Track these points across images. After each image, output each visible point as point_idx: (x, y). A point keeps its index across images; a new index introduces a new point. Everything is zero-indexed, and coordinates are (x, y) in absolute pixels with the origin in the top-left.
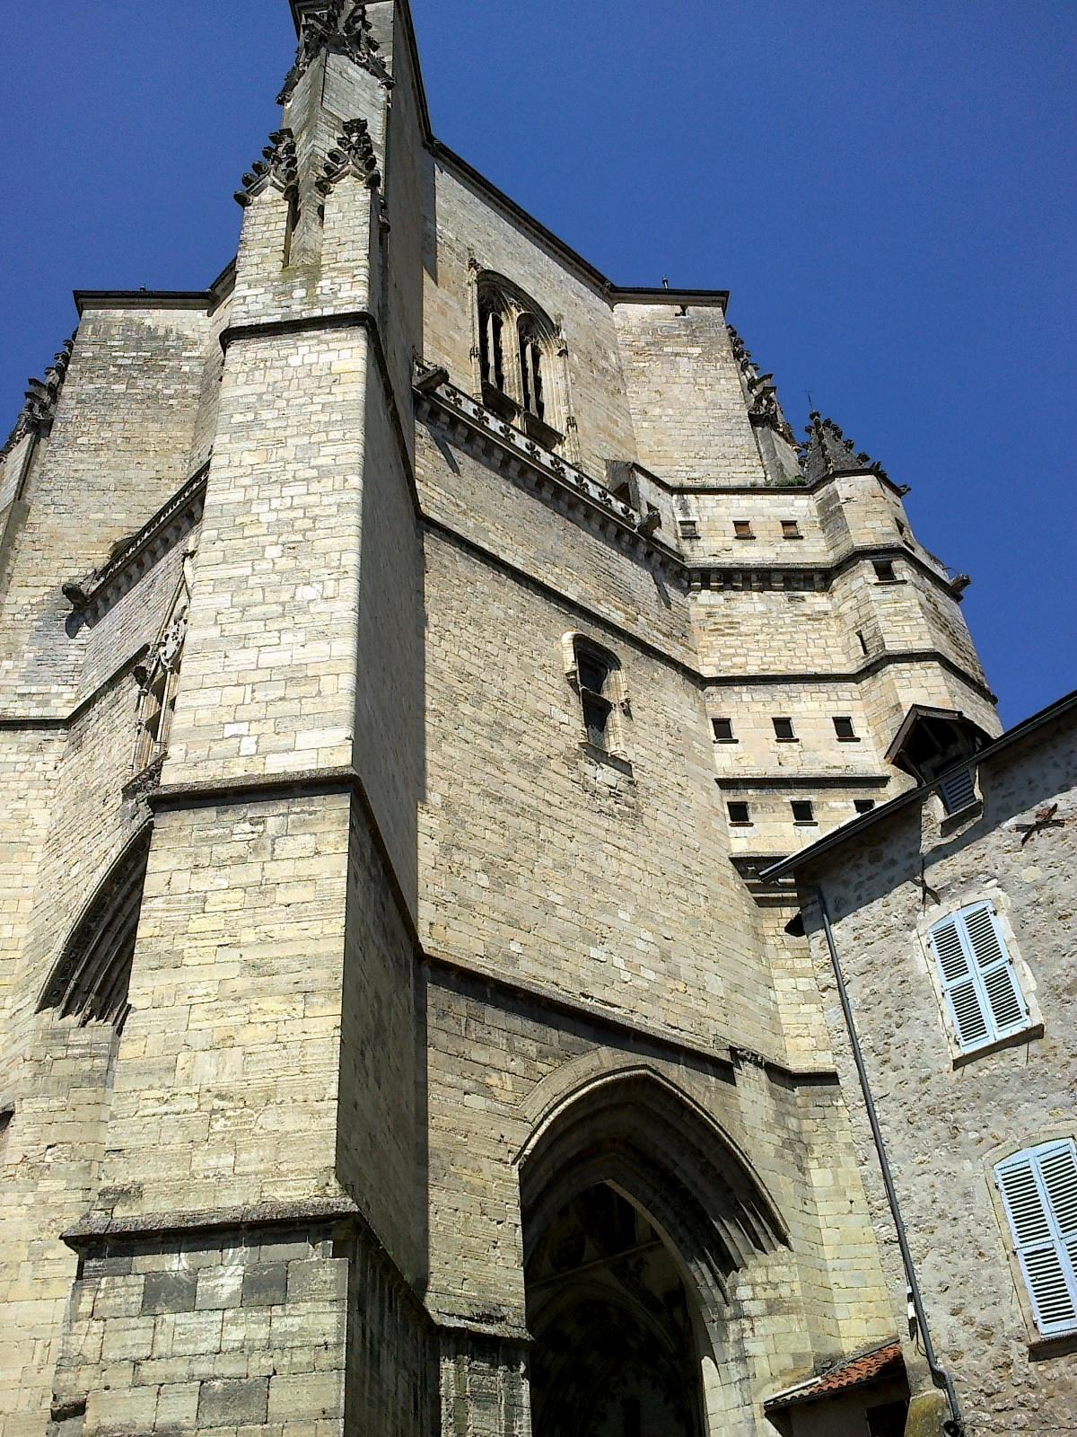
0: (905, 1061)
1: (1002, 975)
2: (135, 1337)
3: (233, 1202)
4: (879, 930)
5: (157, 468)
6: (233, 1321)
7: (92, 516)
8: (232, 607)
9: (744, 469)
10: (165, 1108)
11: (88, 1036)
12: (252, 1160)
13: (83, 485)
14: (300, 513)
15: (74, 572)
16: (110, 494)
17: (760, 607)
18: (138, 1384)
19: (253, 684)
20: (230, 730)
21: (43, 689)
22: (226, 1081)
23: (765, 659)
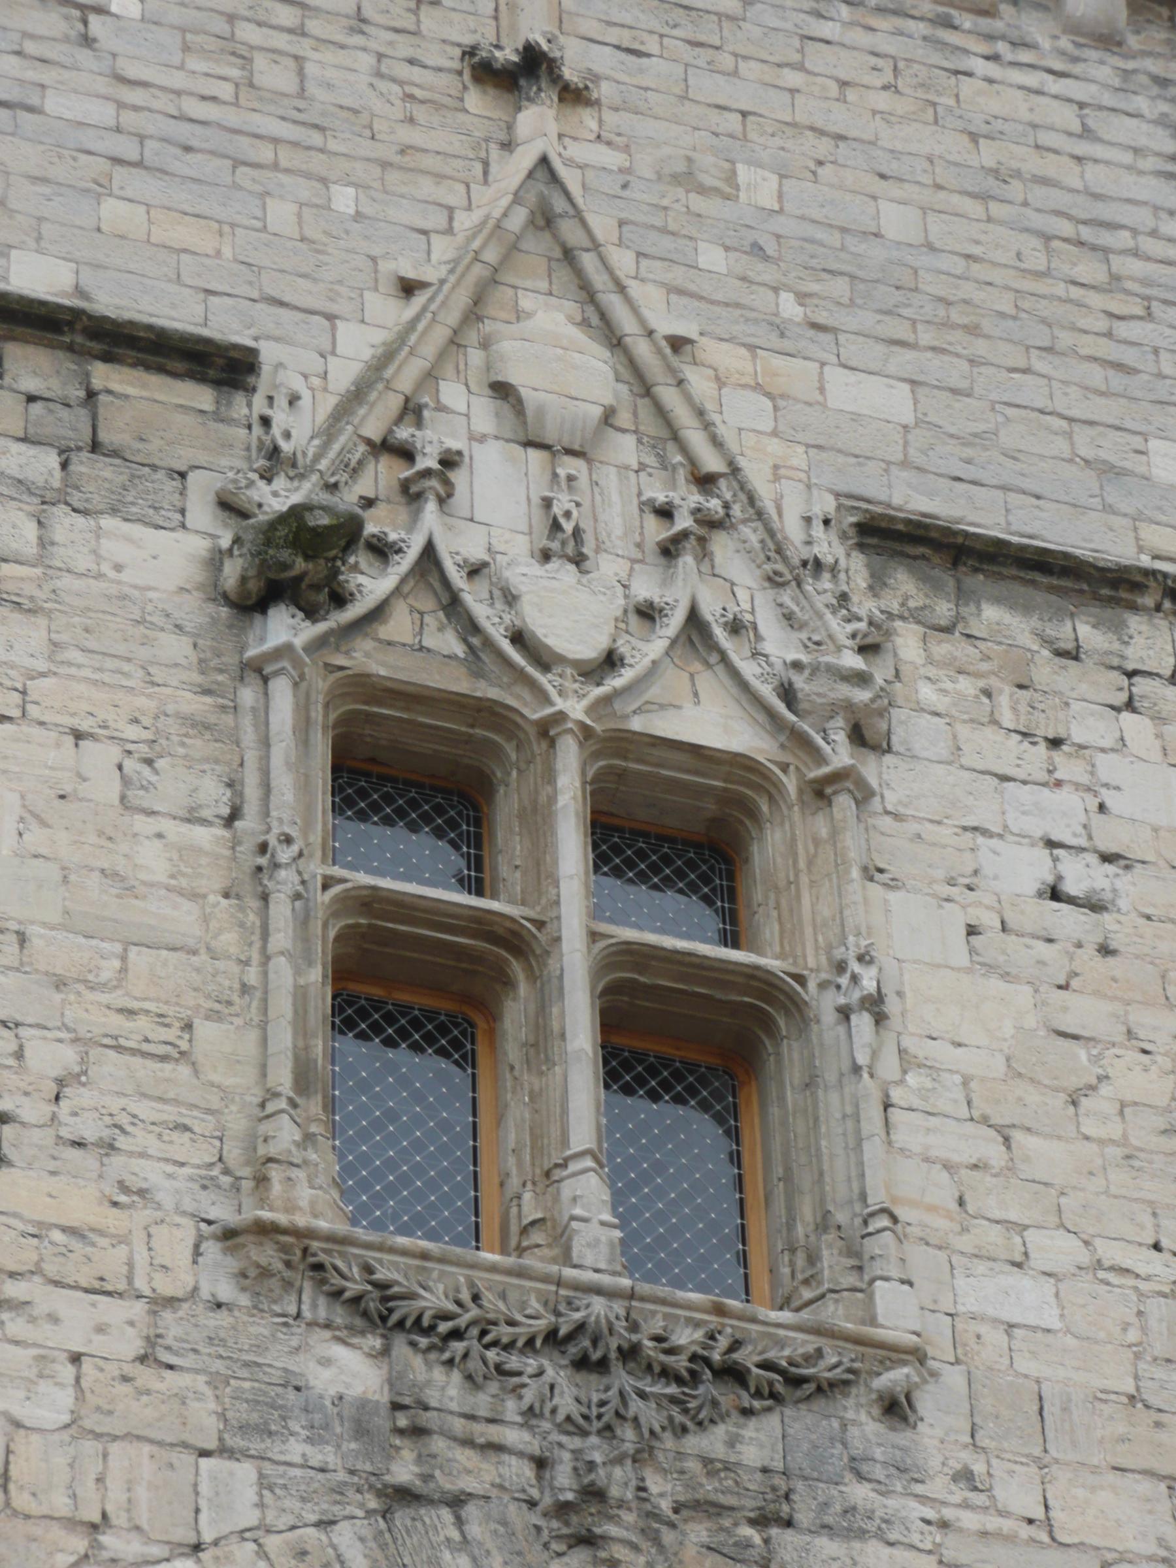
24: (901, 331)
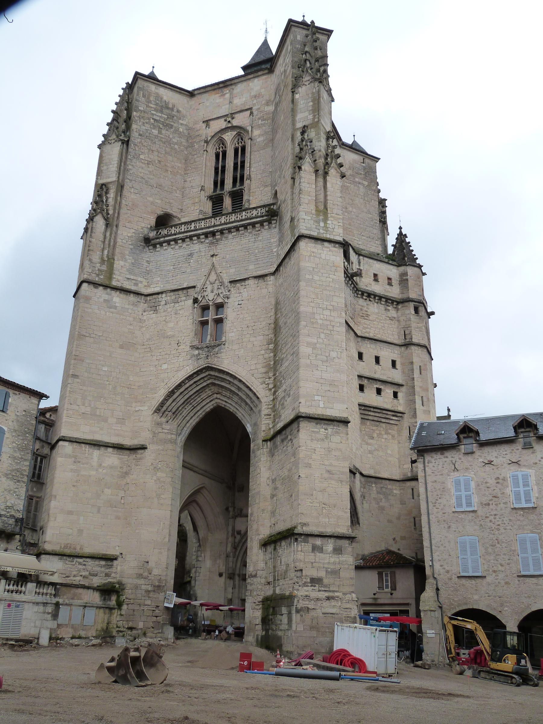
0: (440, 508)
1: (470, 496)
2: (311, 557)
3: (329, 531)
4: (440, 473)
5: (172, 180)
6: (332, 557)
7: (148, 198)
8: (313, 354)
9: (375, 245)
10: (311, 505)
11: (169, 426)
14: (328, 323)
16: (154, 189)
17: (376, 311)
18: (313, 567)
20: (316, 398)
21: (135, 278)
23: (375, 332)
24: (235, 264)
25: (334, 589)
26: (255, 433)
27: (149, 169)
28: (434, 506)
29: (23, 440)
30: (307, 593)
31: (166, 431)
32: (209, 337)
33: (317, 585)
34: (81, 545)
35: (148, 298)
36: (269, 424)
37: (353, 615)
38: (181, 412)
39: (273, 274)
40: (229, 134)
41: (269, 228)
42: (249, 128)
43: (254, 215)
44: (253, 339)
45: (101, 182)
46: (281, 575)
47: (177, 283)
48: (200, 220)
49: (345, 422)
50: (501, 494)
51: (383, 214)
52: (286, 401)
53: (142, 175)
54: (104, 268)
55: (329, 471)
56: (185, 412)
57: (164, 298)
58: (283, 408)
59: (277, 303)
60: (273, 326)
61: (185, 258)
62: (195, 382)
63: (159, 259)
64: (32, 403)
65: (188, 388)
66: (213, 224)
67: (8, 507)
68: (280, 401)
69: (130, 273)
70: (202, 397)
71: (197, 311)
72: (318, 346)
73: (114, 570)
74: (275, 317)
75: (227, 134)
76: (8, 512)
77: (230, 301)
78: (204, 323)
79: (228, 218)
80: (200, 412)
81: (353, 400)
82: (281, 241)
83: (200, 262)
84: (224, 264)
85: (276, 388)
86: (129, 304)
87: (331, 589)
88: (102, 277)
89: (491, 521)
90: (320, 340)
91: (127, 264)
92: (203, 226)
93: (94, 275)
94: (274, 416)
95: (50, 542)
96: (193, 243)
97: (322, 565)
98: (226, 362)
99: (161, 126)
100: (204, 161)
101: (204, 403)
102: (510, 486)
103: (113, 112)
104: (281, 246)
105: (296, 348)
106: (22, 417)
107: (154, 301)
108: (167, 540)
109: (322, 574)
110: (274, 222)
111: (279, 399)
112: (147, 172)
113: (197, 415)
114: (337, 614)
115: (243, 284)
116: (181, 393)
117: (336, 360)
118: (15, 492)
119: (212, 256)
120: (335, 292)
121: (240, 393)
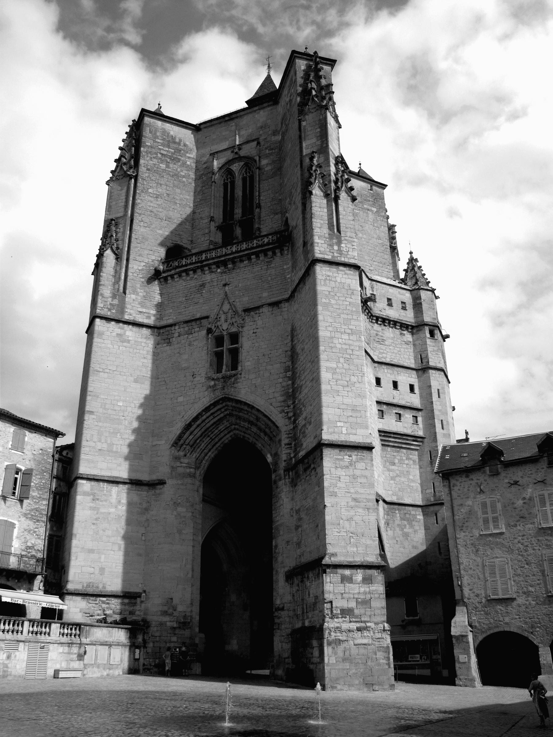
2: (340, 588)
3: (358, 560)
6: (361, 587)
8: (333, 379)
9: (387, 270)
10: (339, 534)
12: (361, 550)
13: (153, 214)
14: (347, 347)
15: (153, 258)
17: (392, 335)
18: (342, 598)
19: (343, 409)
20: (339, 424)
22: (352, 530)
25: (366, 619)
26: (276, 464)
27: (157, 203)
28: (462, 530)
29: (41, 478)
30: (338, 625)
31: (185, 465)
32: (224, 367)
33: (348, 617)
34: (104, 584)
35: (161, 331)
36: (290, 454)
37: (385, 645)
38: (199, 445)
39: (288, 300)
40: (236, 165)
41: (282, 254)
42: (257, 158)
43: (265, 242)
44: (269, 367)
45: (110, 217)
46: (310, 607)
47: (190, 314)
48: (210, 250)
49: (370, 448)
50: (529, 514)
51: (392, 239)
52: (307, 429)
53: (151, 208)
54: (116, 302)
55: (355, 500)
56: (203, 445)
57: (177, 330)
58: (304, 437)
59: (293, 330)
60: (289, 353)
61: (197, 288)
62: (212, 414)
63: (171, 291)
64: (48, 441)
65: (205, 419)
66: (224, 253)
67: (28, 548)
68: (301, 430)
69: (142, 306)
70: (219, 429)
71: (211, 341)
72: (338, 370)
73: (138, 607)
74: (292, 344)
75: (234, 165)
76: (29, 552)
77: (245, 329)
78: (219, 356)
79: (239, 247)
80: (218, 445)
81: (373, 427)
82: (294, 266)
83: (212, 292)
84: (237, 293)
85: (296, 416)
86: (142, 338)
87: (363, 619)
88: (114, 311)
89: (519, 542)
90: (340, 365)
91: (139, 298)
92: (214, 256)
93: (106, 310)
94: (295, 445)
95: (72, 582)
96: (204, 274)
97: (352, 596)
98: (243, 392)
99: (168, 160)
100: (213, 193)
101: (222, 434)
102: (536, 505)
103: (121, 148)
104: (295, 271)
105: (315, 374)
106: (39, 456)
107: (167, 333)
108: (190, 575)
109: (352, 604)
110: (286, 248)
111: (300, 427)
112: (156, 206)
113: (215, 448)
114: (369, 645)
115: (257, 312)
116: (198, 426)
117: (357, 385)
118: (35, 532)
119: (225, 285)
120: (352, 315)
121: (259, 423)
